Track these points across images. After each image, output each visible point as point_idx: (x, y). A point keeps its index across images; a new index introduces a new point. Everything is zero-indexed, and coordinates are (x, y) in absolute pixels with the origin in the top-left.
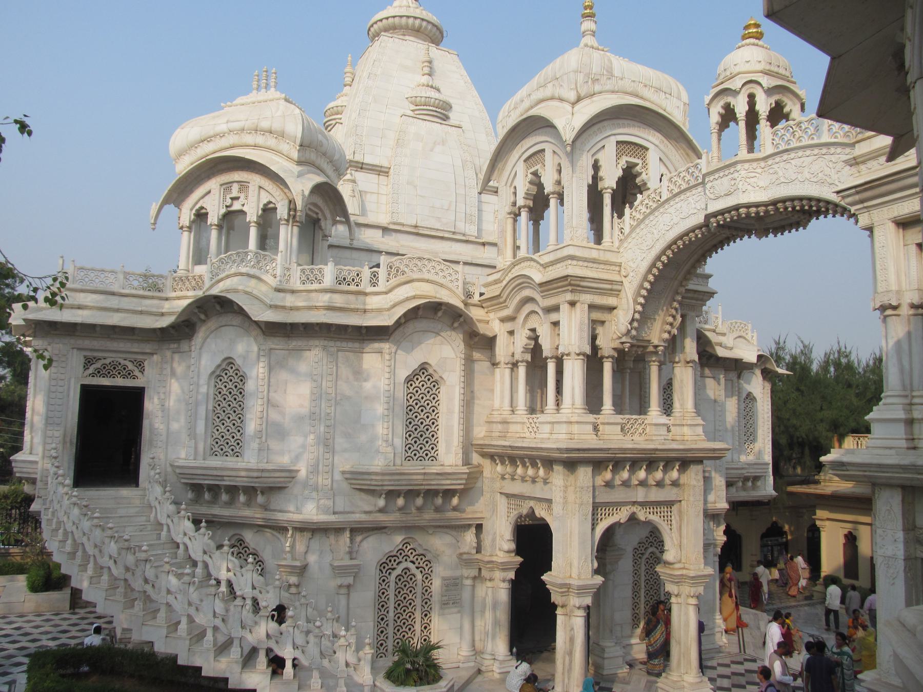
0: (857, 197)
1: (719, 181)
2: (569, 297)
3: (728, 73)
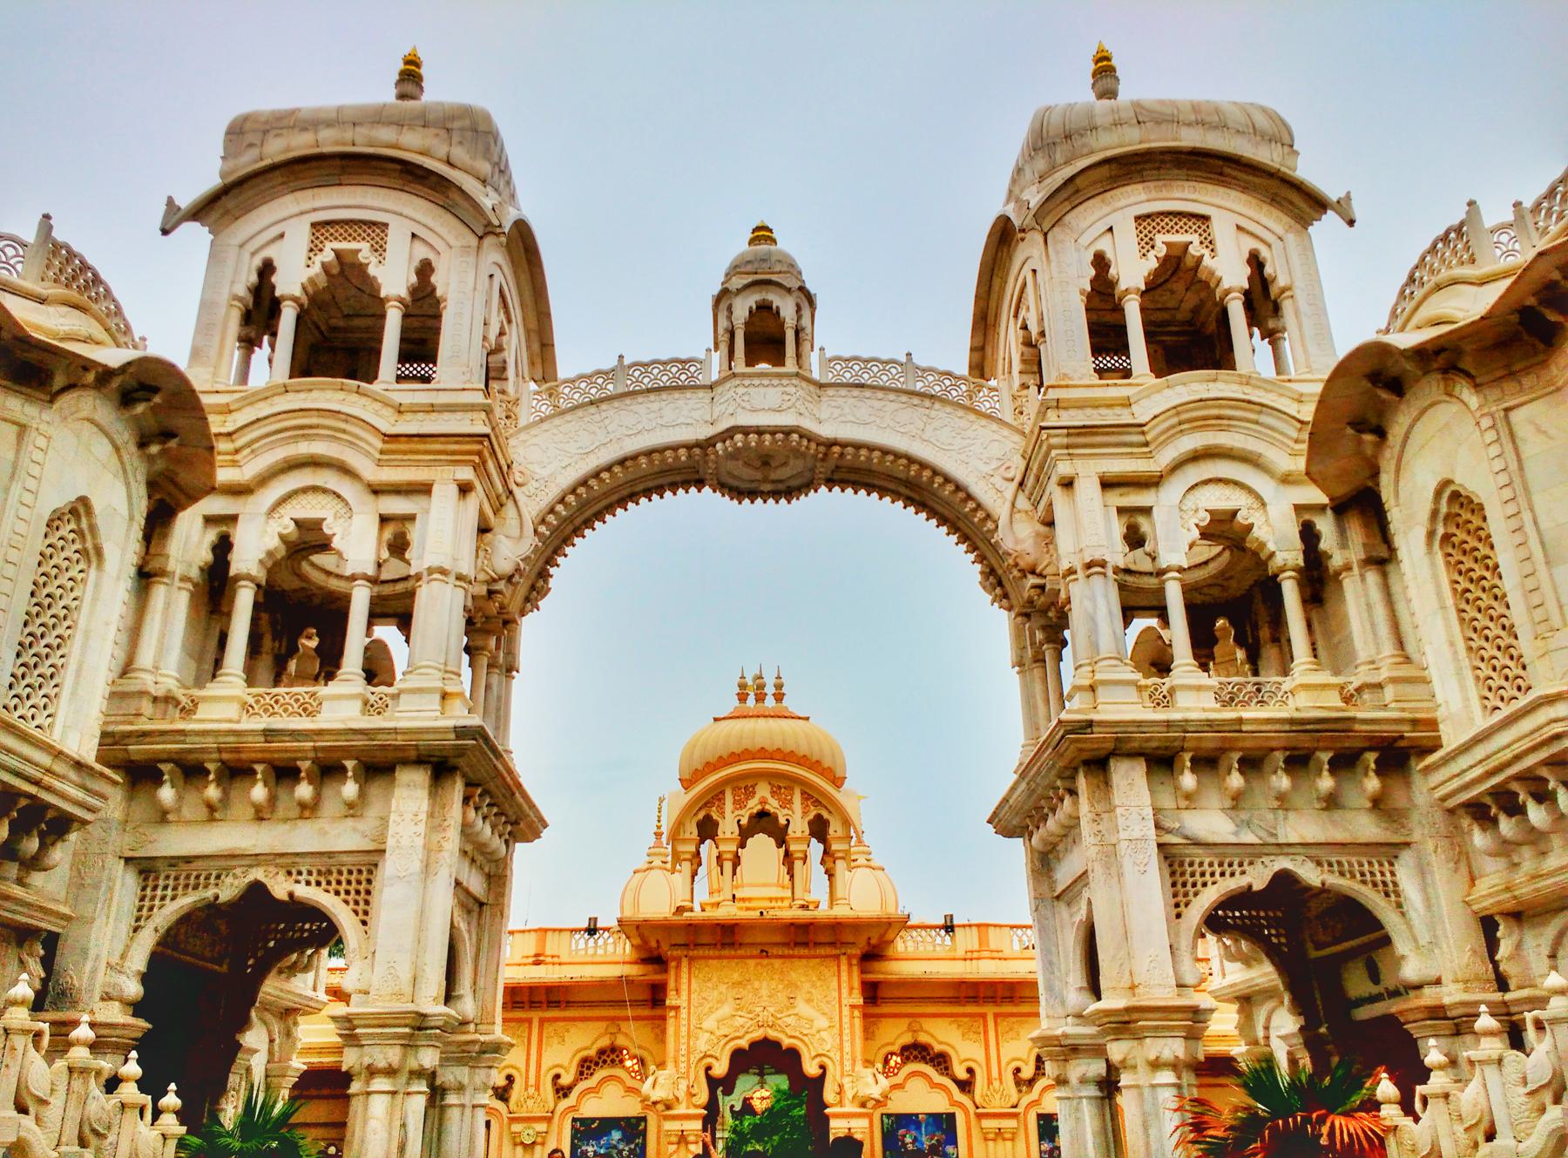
1: (761, 389)
2: (466, 473)
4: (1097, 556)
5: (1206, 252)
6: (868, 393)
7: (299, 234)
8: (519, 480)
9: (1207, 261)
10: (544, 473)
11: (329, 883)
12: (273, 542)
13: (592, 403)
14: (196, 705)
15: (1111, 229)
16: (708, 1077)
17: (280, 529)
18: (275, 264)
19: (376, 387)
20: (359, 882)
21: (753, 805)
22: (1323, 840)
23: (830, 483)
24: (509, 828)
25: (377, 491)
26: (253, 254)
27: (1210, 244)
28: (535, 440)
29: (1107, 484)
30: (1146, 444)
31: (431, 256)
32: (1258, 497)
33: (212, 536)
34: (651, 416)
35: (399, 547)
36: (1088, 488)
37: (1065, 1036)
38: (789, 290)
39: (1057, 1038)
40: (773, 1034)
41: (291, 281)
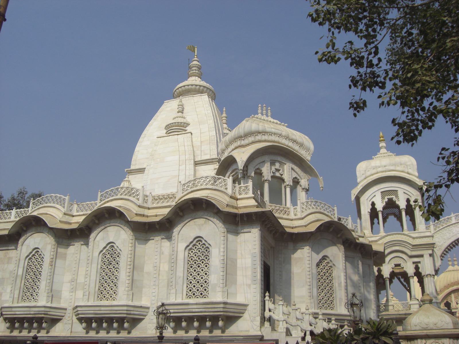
10: (440, 244)
18: (375, 203)
26: (370, 201)
31: (409, 197)
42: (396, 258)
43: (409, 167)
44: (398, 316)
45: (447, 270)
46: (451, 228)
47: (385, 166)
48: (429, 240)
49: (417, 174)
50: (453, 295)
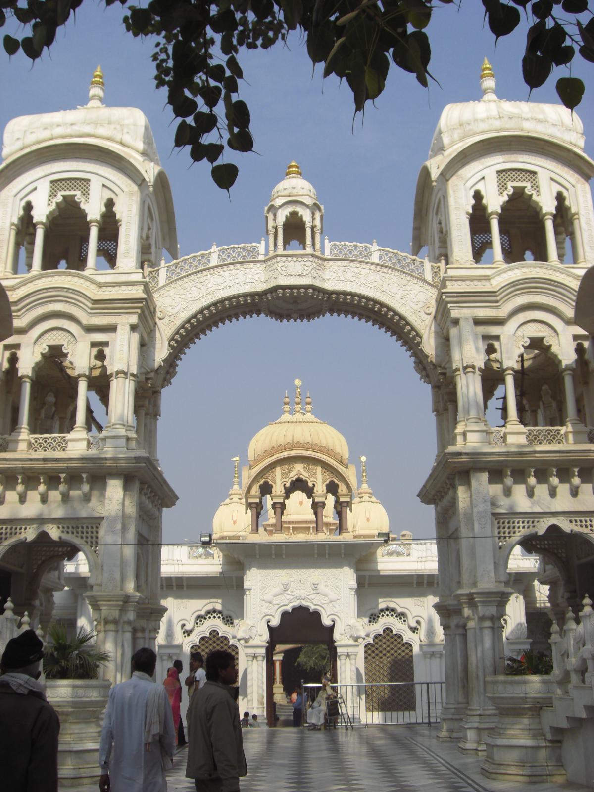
0: (455, 299)
1: (292, 263)
3: (294, 191)
4: (470, 363)
5: (534, 192)
6: (351, 264)
7: (44, 187)
8: (160, 316)
9: (535, 198)
10: (174, 311)
11: (78, 533)
12: (38, 358)
13: (199, 272)
14: (8, 443)
15: (483, 178)
16: (269, 626)
17: (41, 351)
18: (33, 204)
19: (86, 273)
20: (92, 532)
21: (293, 475)
22: (572, 510)
23: (332, 311)
24: (160, 502)
25: (89, 329)
26: (22, 200)
27: (536, 187)
28: (168, 294)
29: (478, 322)
30: (497, 302)
31: (113, 196)
32: (555, 331)
33: (8, 354)
34: (232, 278)
35: (101, 356)
36: (467, 327)
37: (449, 605)
38: (307, 206)
39: (445, 606)
40: (305, 603)
41: (40, 214)
42: (55, 332)
43: (125, 130)
44: (27, 465)
45: (279, 420)
46: (205, 278)
47: (72, 124)
48: (135, 291)
49: (140, 146)
50: (278, 470)
